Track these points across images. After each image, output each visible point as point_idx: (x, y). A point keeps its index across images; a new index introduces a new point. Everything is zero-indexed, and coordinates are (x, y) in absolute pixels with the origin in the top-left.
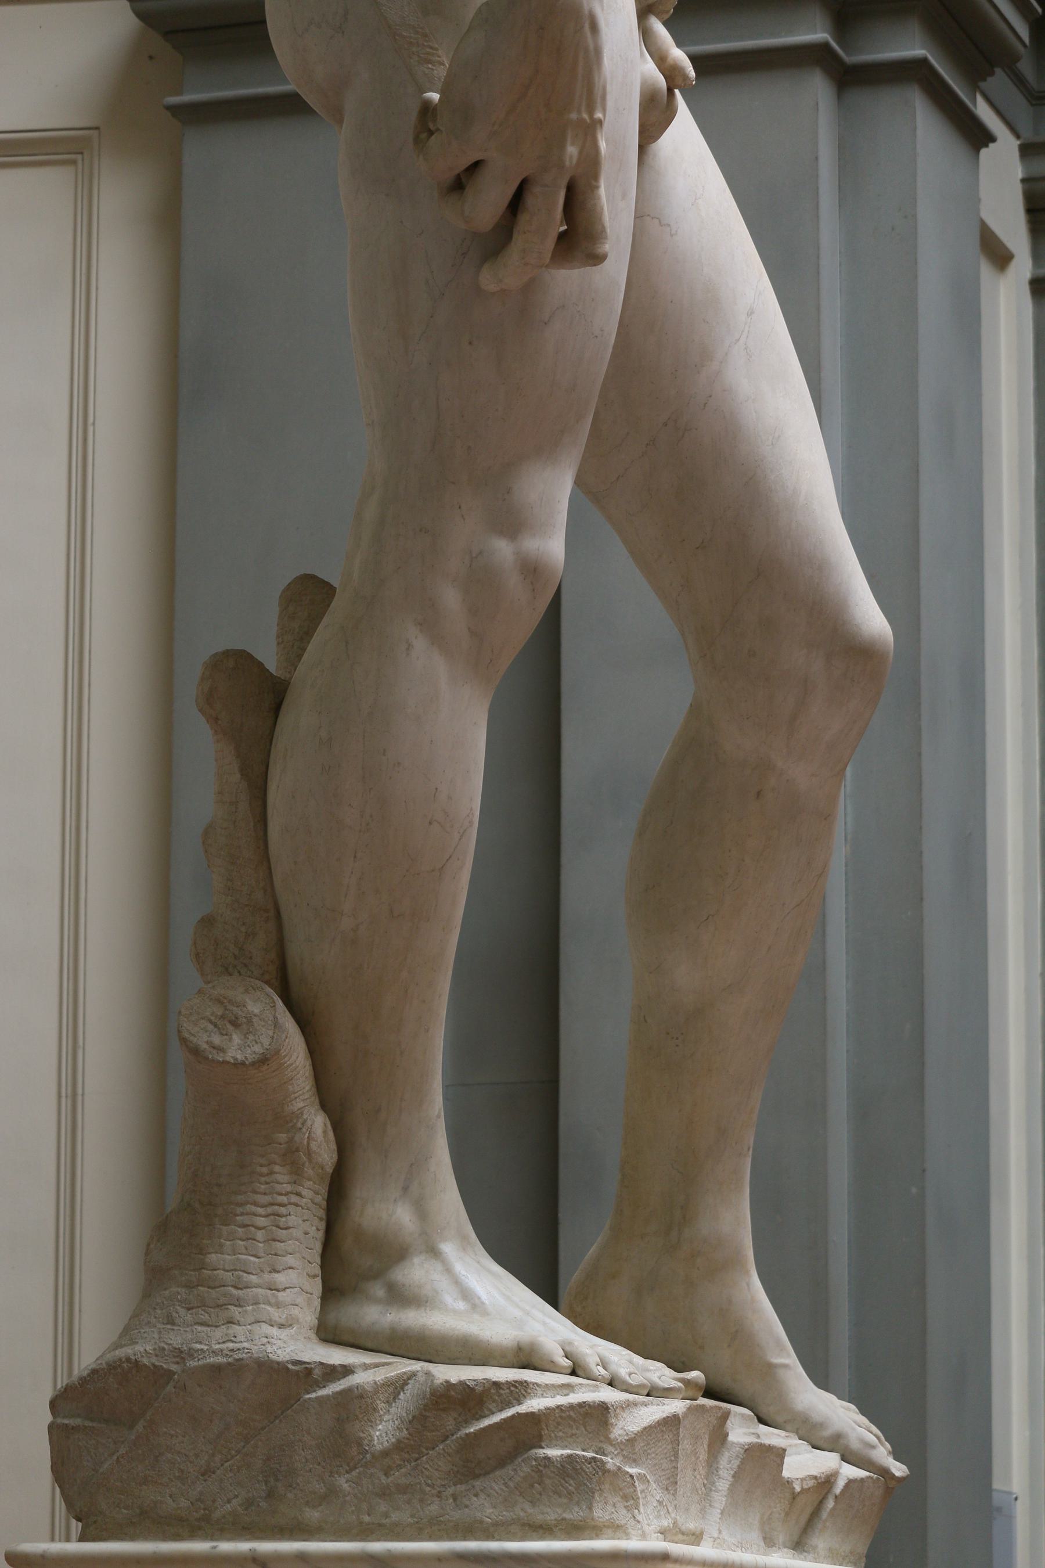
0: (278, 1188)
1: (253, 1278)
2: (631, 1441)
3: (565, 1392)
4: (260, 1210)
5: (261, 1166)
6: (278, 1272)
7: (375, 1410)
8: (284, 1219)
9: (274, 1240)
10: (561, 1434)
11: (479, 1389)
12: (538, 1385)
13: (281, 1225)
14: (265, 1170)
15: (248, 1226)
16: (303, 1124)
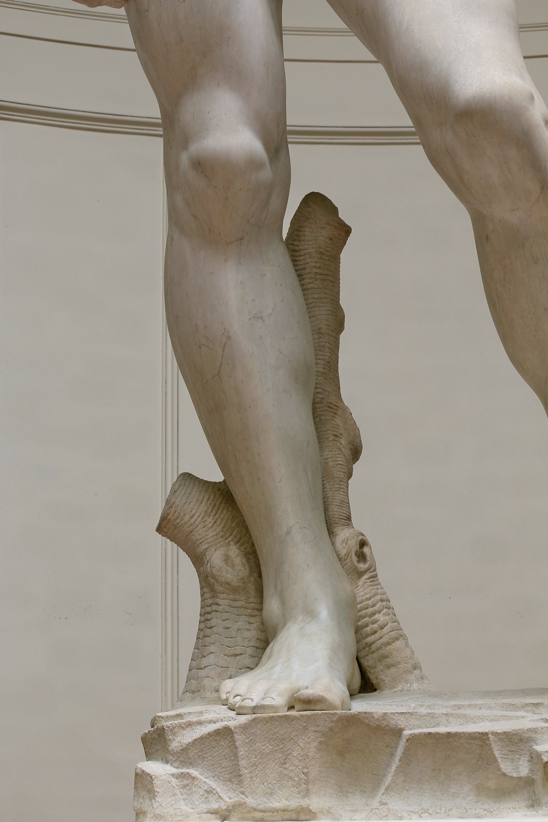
2: (185, 750)
6: (205, 657)
8: (209, 622)
9: (205, 636)
10: (153, 750)
12: (162, 717)
13: (208, 625)
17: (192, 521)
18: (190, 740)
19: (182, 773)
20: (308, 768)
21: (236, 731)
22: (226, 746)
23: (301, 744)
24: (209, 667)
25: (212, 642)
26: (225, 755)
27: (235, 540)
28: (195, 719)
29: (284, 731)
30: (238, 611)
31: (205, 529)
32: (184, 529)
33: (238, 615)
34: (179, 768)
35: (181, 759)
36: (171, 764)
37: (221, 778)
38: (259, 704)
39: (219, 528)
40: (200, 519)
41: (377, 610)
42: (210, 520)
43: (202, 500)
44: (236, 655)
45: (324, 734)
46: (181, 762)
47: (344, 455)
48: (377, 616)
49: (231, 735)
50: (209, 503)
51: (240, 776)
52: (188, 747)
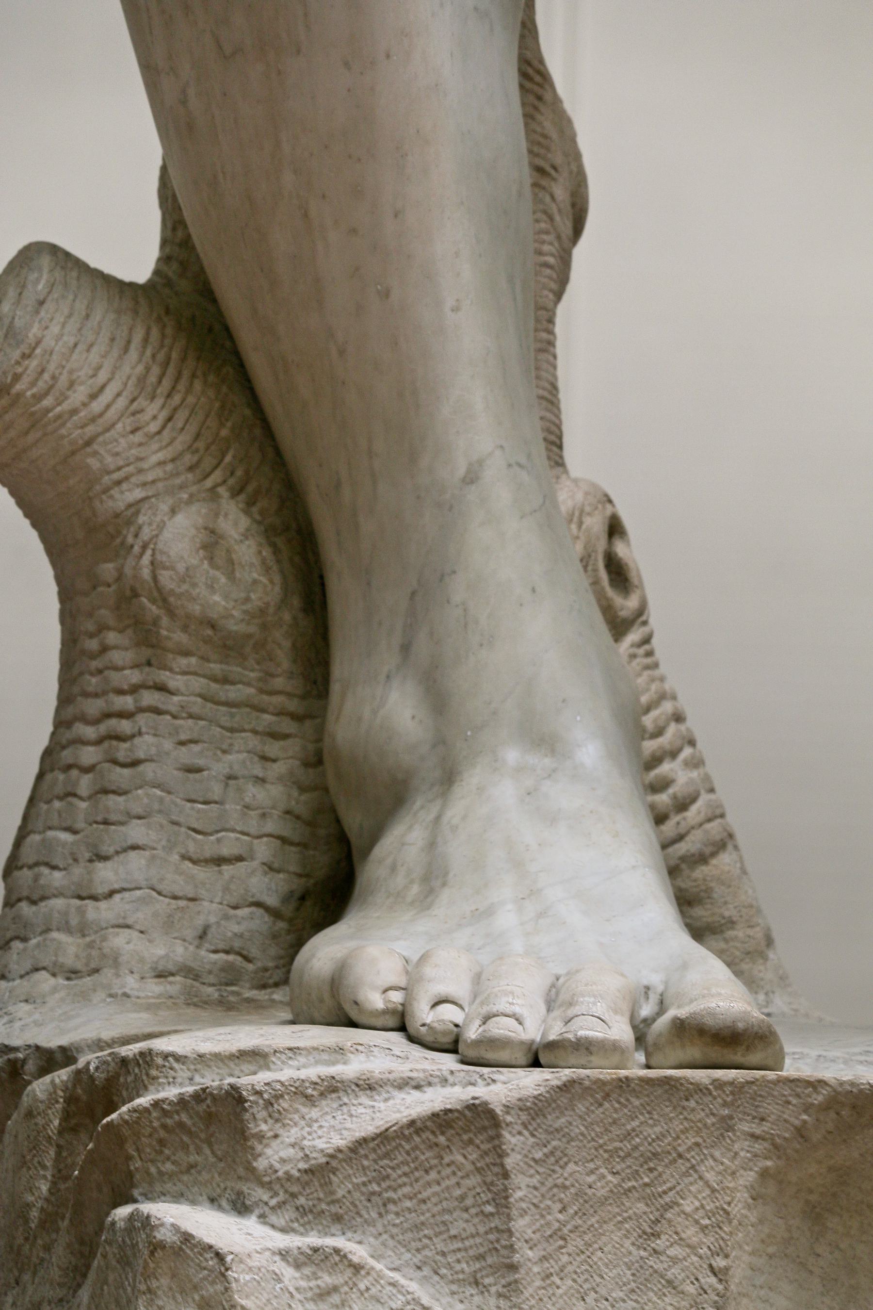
0: (116, 678)
1: (57, 878)
2: (320, 1172)
3: (246, 1067)
4: (90, 732)
5: (91, 636)
6: (106, 858)
9: (106, 792)
10: (169, 1167)
11: (101, 1076)
12: (178, 1058)
13: (121, 756)
14: (93, 645)
15: (69, 767)
16: (136, 536)
17: (96, 406)
18: (339, 1141)
19: (316, 1250)
20: (727, 1256)
21: (509, 1119)
22: (469, 1167)
23: (710, 1176)
24: (126, 895)
25: (138, 810)
26: (462, 1198)
27: (231, 481)
28: (313, 1072)
29: (658, 1129)
30: (232, 715)
31: (138, 438)
32: (63, 431)
33: (232, 730)
34: (293, 1230)
35: (302, 1200)
36: (262, 1216)
37: (443, 1271)
38: (570, 1036)
39: (183, 439)
40: (121, 402)
41: (668, 747)
42: (153, 411)
43: (129, 342)
44: (220, 861)
45: (776, 1146)
46: (302, 1211)
47: (559, 237)
48: (666, 768)
49: (491, 1132)
50: (149, 352)
51: (513, 1268)
52: (334, 1163)
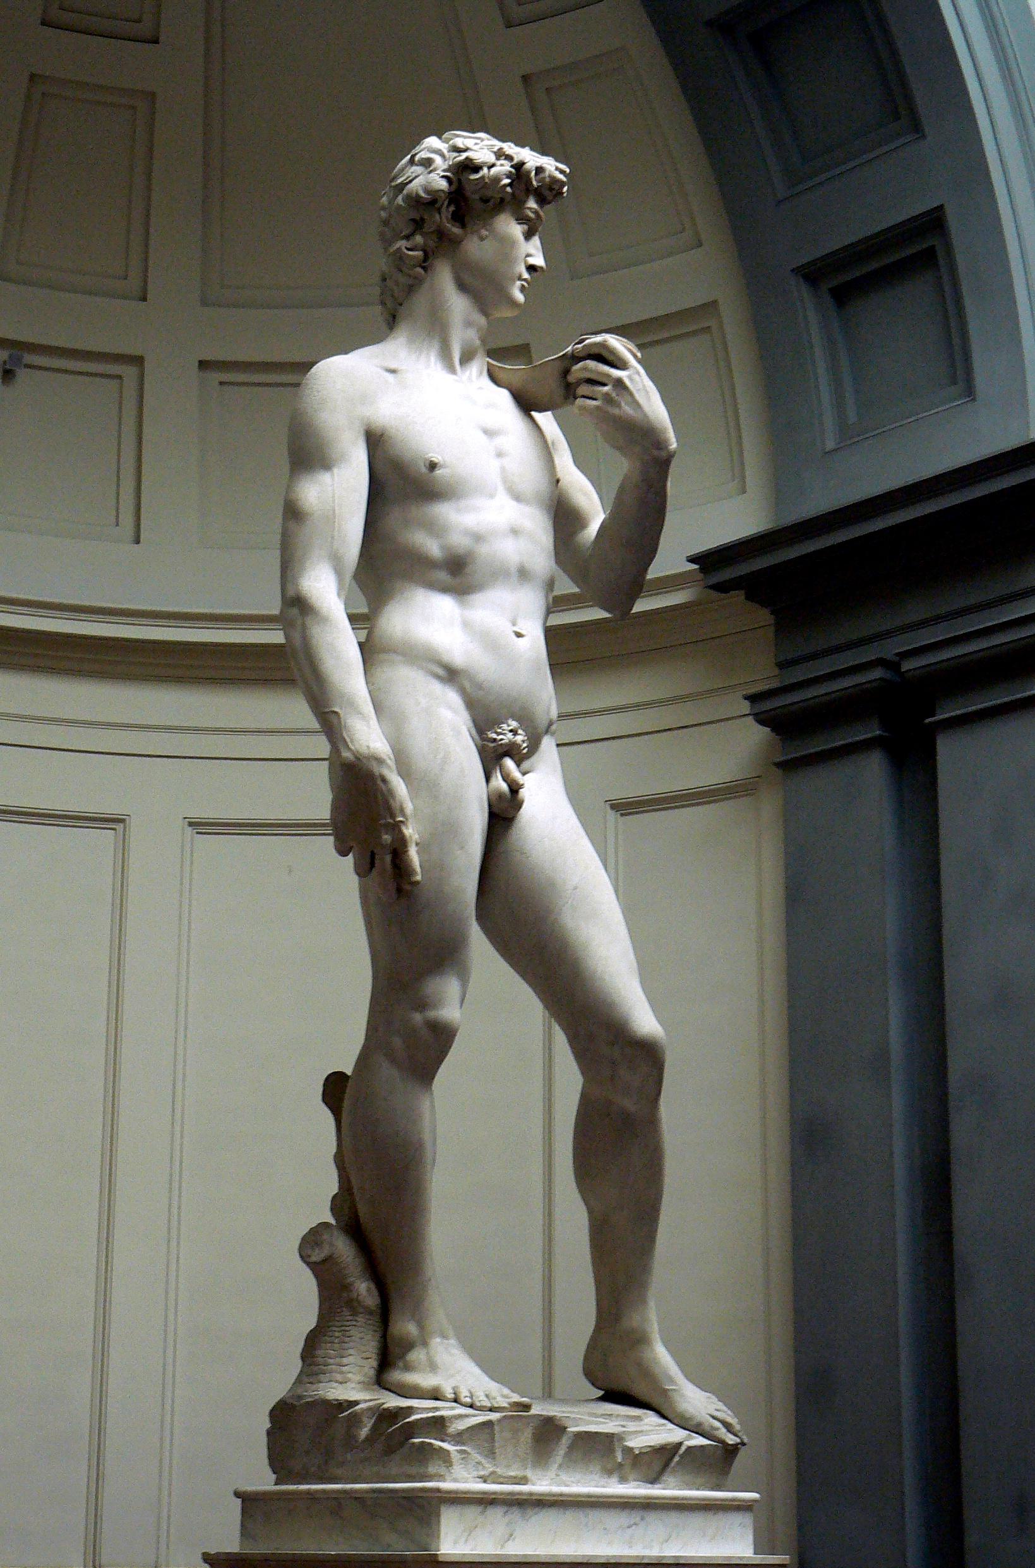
7: (361, 1422)
